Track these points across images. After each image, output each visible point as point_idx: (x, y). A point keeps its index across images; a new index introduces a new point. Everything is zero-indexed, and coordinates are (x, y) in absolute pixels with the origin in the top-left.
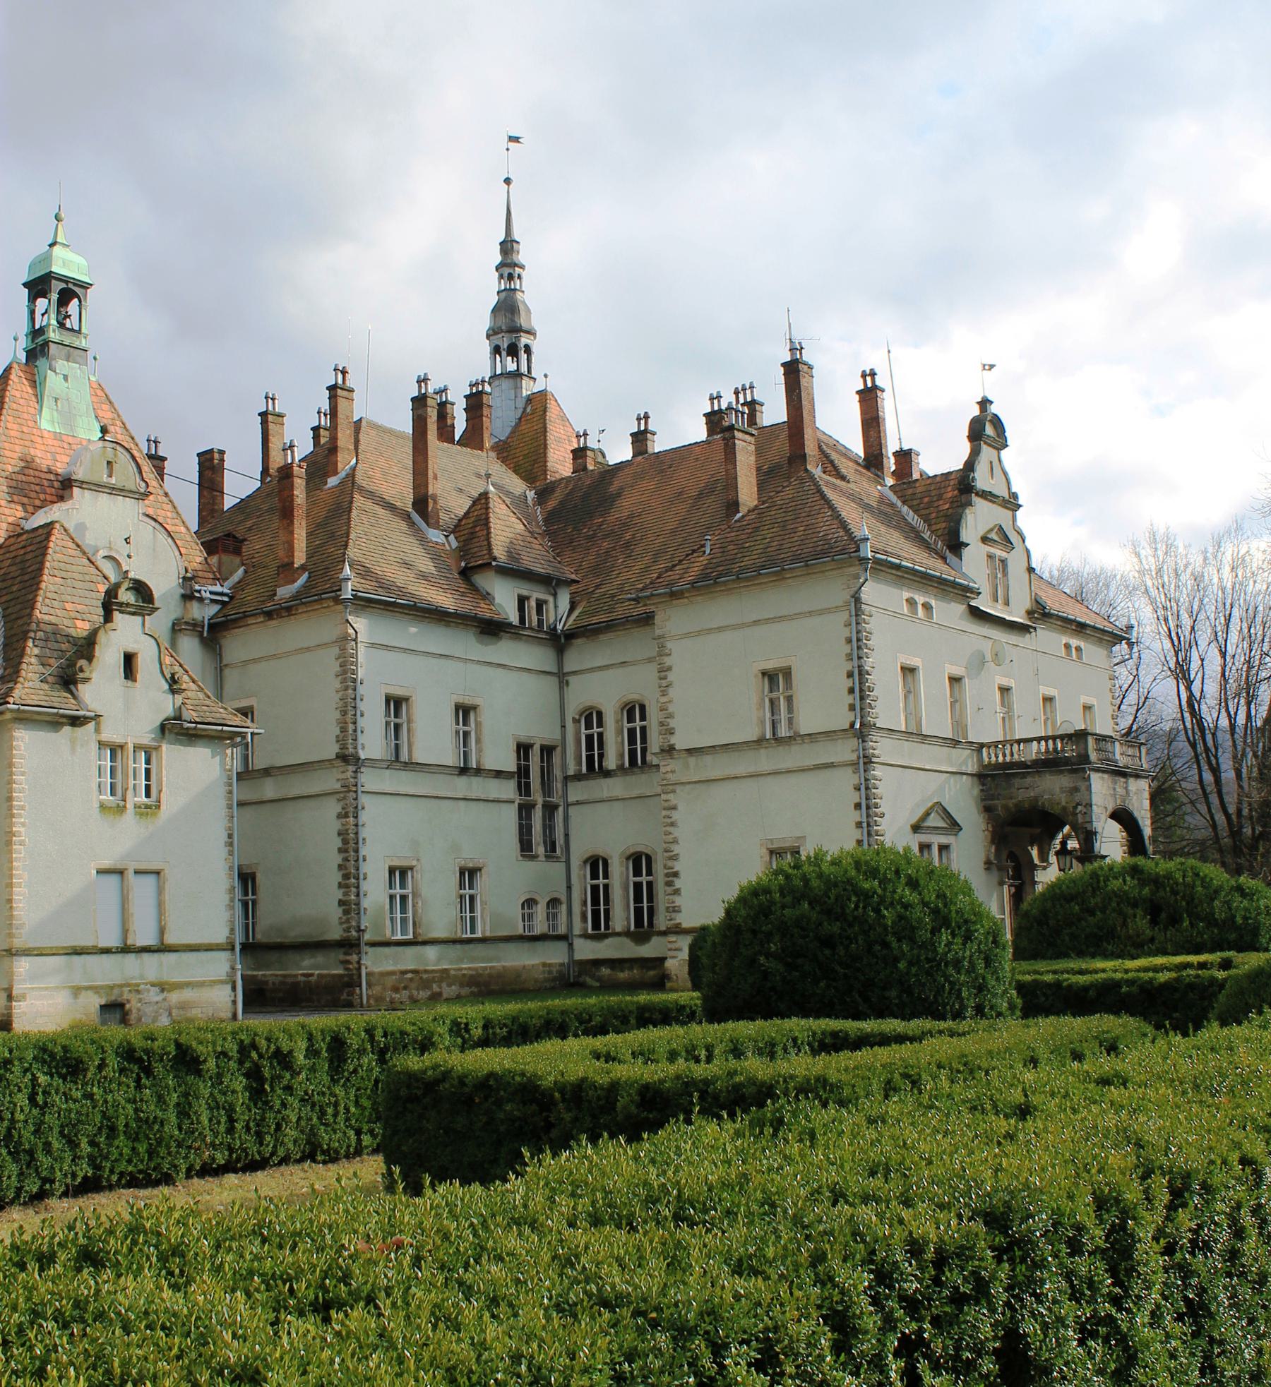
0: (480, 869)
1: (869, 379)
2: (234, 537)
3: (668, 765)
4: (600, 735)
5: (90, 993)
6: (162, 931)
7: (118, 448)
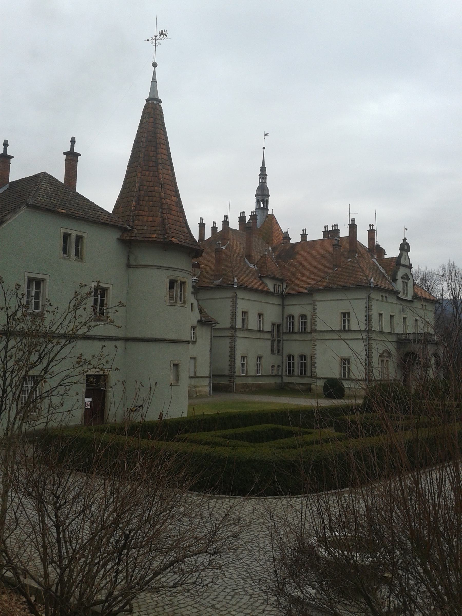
0: (262, 357)
1: (371, 227)
3: (314, 334)
4: (293, 322)
6: (195, 373)
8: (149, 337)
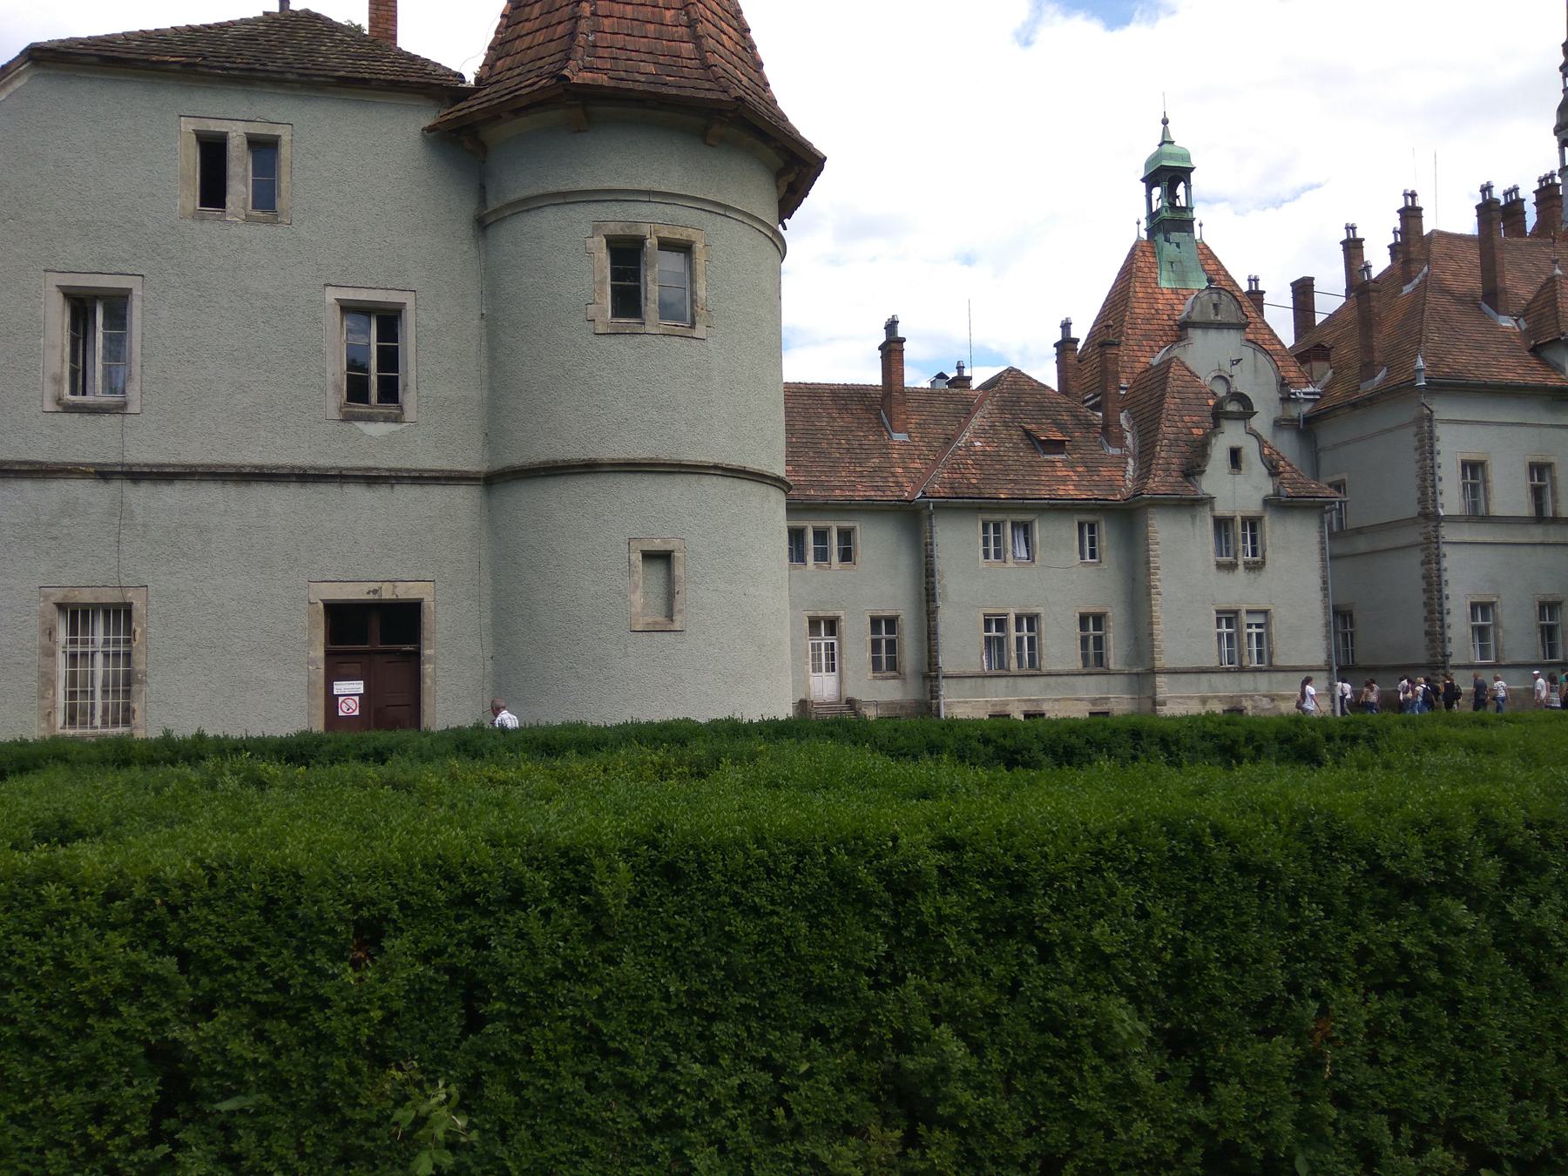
2: (1323, 346)
5: (1215, 701)
7: (1222, 292)
8: (543, 458)
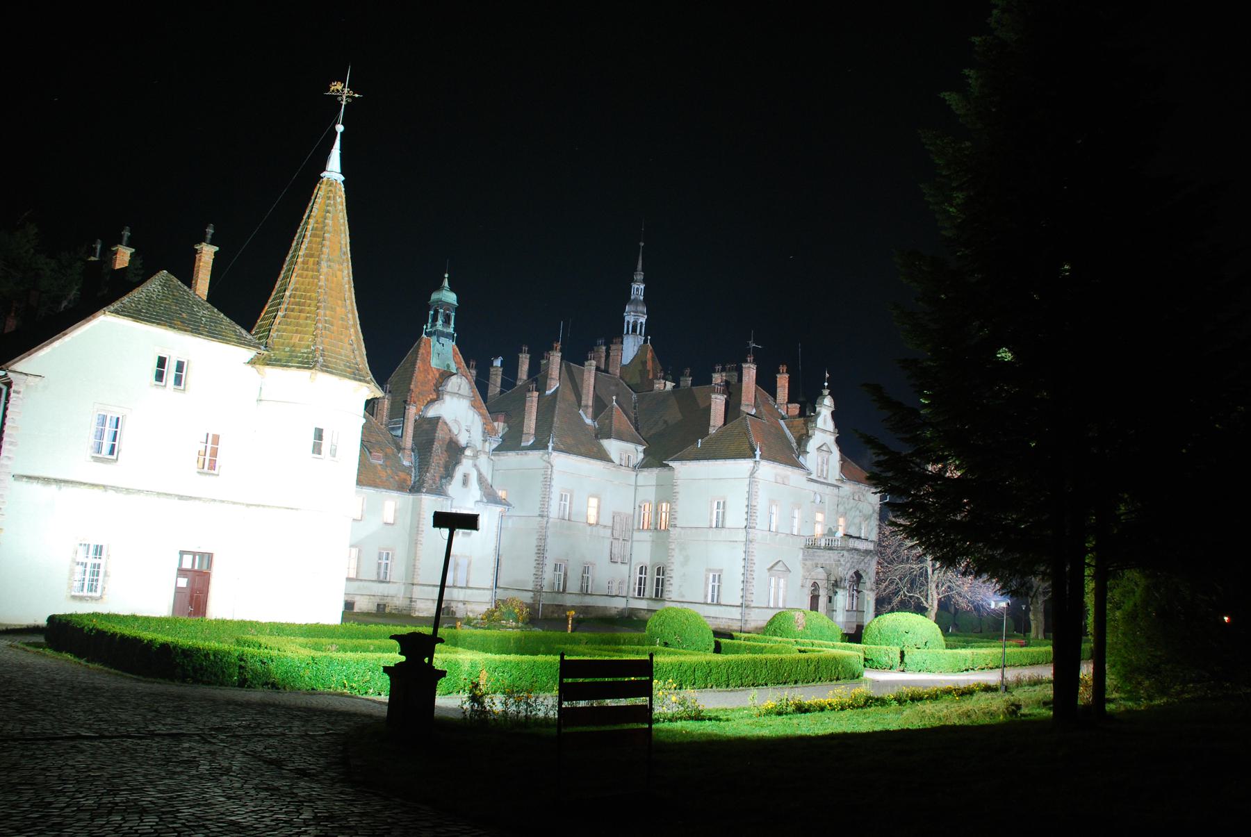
6: (467, 582)
